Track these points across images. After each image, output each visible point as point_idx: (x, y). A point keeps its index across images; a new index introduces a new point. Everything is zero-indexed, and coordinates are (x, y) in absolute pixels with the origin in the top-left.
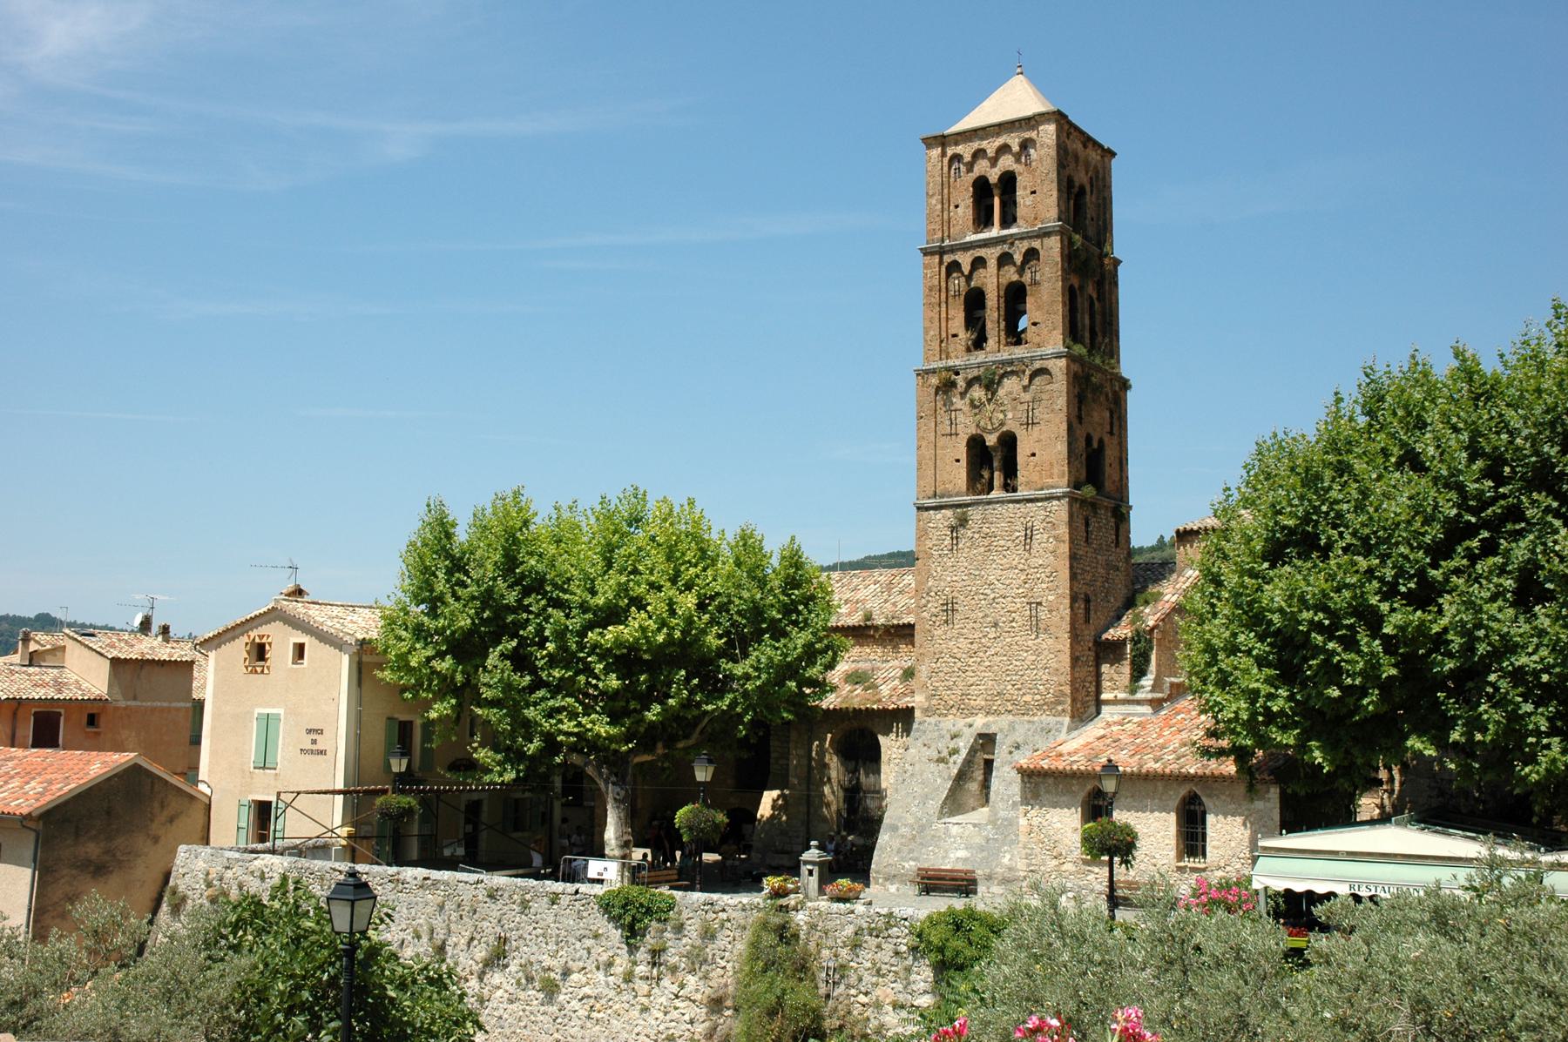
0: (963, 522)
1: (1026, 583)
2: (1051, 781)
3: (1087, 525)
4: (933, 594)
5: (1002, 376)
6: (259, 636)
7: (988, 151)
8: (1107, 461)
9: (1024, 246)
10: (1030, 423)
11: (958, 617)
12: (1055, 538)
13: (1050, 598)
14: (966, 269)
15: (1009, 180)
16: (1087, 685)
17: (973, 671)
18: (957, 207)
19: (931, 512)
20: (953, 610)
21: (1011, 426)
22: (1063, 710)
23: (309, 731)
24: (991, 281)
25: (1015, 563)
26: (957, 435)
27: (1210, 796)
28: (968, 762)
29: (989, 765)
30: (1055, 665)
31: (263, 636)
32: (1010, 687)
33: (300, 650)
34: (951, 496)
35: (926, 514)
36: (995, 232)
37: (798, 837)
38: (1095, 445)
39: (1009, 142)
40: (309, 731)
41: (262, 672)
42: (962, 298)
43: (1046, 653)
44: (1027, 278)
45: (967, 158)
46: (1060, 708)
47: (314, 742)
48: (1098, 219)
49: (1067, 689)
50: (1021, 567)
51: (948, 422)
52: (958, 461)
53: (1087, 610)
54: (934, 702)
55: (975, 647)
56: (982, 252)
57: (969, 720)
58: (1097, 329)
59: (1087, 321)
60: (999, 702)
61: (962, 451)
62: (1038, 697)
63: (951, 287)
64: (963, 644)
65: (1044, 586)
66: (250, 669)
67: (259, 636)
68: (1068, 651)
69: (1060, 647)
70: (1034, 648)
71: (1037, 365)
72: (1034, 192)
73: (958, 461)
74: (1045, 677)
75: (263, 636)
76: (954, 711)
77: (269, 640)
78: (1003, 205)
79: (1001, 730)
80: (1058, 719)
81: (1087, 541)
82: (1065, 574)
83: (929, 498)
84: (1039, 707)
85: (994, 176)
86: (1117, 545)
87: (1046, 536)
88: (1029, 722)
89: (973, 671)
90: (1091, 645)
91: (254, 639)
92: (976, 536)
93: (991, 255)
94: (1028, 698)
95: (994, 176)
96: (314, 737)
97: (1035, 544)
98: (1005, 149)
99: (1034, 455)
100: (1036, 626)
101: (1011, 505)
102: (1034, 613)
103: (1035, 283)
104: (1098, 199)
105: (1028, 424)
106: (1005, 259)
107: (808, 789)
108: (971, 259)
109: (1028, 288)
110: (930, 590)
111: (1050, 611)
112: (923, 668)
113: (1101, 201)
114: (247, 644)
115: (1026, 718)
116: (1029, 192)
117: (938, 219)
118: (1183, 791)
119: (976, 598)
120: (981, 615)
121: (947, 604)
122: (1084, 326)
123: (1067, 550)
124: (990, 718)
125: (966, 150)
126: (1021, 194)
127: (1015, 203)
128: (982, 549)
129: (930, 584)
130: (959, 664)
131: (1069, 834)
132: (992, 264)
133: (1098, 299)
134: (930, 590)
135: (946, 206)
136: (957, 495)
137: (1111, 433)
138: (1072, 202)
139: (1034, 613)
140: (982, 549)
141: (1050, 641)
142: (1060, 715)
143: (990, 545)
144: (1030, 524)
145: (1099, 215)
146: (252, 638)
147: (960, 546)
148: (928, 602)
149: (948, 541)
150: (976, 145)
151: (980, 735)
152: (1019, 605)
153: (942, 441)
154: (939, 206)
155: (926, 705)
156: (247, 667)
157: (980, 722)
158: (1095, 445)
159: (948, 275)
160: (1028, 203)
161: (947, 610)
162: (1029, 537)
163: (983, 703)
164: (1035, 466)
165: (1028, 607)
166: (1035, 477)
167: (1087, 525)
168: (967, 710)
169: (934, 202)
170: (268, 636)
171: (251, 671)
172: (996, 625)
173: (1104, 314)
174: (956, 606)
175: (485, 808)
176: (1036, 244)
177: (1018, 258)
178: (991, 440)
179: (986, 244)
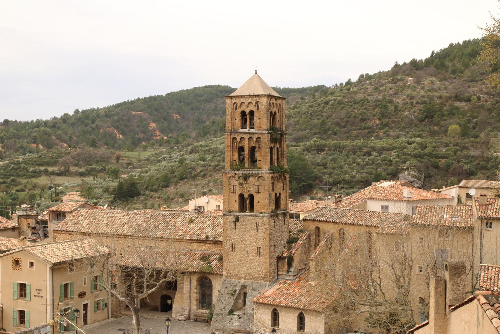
0: (237, 220)
1: (256, 241)
2: (263, 305)
3: (275, 222)
4: (228, 241)
5: (249, 177)
6: (17, 258)
7: (246, 103)
8: (282, 199)
9: (257, 136)
10: (258, 192)
11: (236, 249)
12: (265, 229)
13: (264, 246)
14: (239, 140)
15: (252, 113)
16: (274, 270)
17: (240, 266)
18: (236, 119)
19: (228, 216)
20: (234, 247)
22: (267, 280)
23: (37, 290)
25: (253, 234)
26: (235, 193)
27: (306, 314)
28: (239, 294)
29: (245, 294)
30: (264, 266)
31: (18, 258)
32: (251, 272)
33: (32, 264)
34: (233, 212)
35: (226, 217)
36: (247, 130)
37: (187, 310)
38: (278, 196)
39: (252, 102)
40: (37, 290)
41: (19, 270)
42: (237, 149)
43: (262, 262)
44: (257, 145)
45: (239, 104)
46: (266, 279)
47: (39, 293)
48: (280, 121)
49: (268, 274)
50: (255, 236)
51: (233, 189)
52: (236, 201)
53: (275, 248)
54: (229, 274)
55: (241, 259)
56: (243, 136)
57: (239, 280)
58: (279, 157)
59: (276, 157)
60: (248, 276)
61: (237, 198)
62: (259, 275)
63: (234, 146)
64: (237, 257)
65: (262, 243)
66: (14, 268)
67: (17, 258)
68: (268, 262)
69: (266, 261)
70: (259, 261)
71: (260, 175)
72: (260, 119)
73: (236, 201)
74: (262, 270)
75: (18, 258)
76: (235, 277)
77: (21, 260)
78: (250, 119)
79: (249, 285)
80: (266, 282)
81: (275, 227)
82: (268, 240)
83: (227, 212)
84: (260, 278)
85: (247, 111)
86: (284, 225)
87: (262, 228)
88: (257, 283)
89: (240, 266)
90: (276, 258)
91: (15, 259)
92: (241, 225)
93: (247, 137)
94: (257, 275)
95: (247, 111)
96: (39, 292)
97: (259, 230)
98: (250, 103)
99: (259, 202)
100: (259, 254)
101: (252, 217)
102: (259, 250)
103: (259, 148)
104: (280, 114)
105: (257, 192)
106: (250, 138)
107: (190, 295)
108: (240, 138)
110: (227, 240)
111: (263, 250)
112: (226, 264)
113: (281, 115)
114: (12, 260)
115: (256, 281)
117: (230, 123)
118: (299, 312)
119: (241, 244)
120: (242, 249)
121: (233, 245)
122: (275, 158)
123: (268, 233)
124: (246, 280)
125: (239, 101)
126: (256, 119)
127: (254, 119)
128: (243, 230)
129: (227, 238)
130: (236, 264)
131: (268, 321)
132: (247, 140)
133: (280, 147)
134: (227, 240)
135: (232, 119)
136: (236, 212)
137: (283, 190)
138: (272, 119)
139: (259, 250)
140: (243, 230)
141: (263, 259)
142: (266, 281)
143: (245, 228)
144: (257, 223)
145: (280, 119)
146: (14, 258)
147: (237, 228)
148: (227, 244)
149: (233, 226)
150: (242, 100)
151: (242, 286)
152: (254, 248)
153: (231, 194)
154: (230, 119)
155: (226, 275)
156: (13, 268)
157: (242, 281)
158: (278, 196)
159: (233, 142)
160: (258, 122)
161: (232, 247)
162: (257, 227)
163: (243, 276)
164: (259, 205)
165: (257, 248)
166: (259, 209)
167: (275, 222)
168: (239, 278)
169: (228, 118)
170: (20, 259)
171: (15, 269)
172: (247, 252)
173: (282, 151)
174: (235, 246)
175: (89, 305)
176: (260, 136)
177: (255, 139)
178: (246, 196)
179: (245, 133)
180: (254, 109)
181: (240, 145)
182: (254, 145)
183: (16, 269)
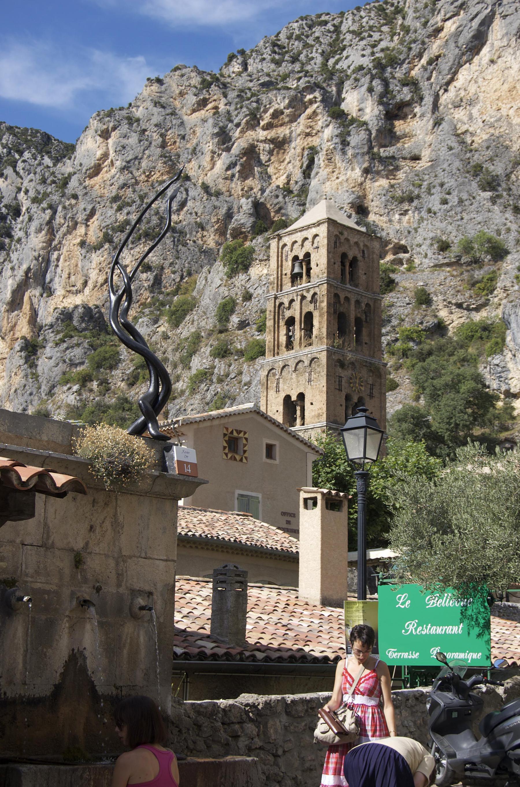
6: (236, 430)
18: (335, 263)
21: (363, 395)
23: (284, 514)
24: (352, 313)
31: (241, 432)
33: (270, 449)
40: (284, 514)
41: (241, 460)
44: (363, 317)
47: (288, 522)
56: (349, 295)
66: (230, 456)
67: (236, 430)
72: (365, 274)
73: (341, 405)
75: (241, 432)
77: (246, 436)
91: (232, 432)
96: (289, 519)
98: (356, 243)
103: (366, 321)
109: (364, 323)
114: (225, 435)
116: (364, 272)
146: (230, 430)
156: (226, 455)
170: (245, 433)
171: (231, 458)
177: (363, 305)
180: (359, 256)
181: (342, 309)
182: (359, 315)
183: (235, 459)
